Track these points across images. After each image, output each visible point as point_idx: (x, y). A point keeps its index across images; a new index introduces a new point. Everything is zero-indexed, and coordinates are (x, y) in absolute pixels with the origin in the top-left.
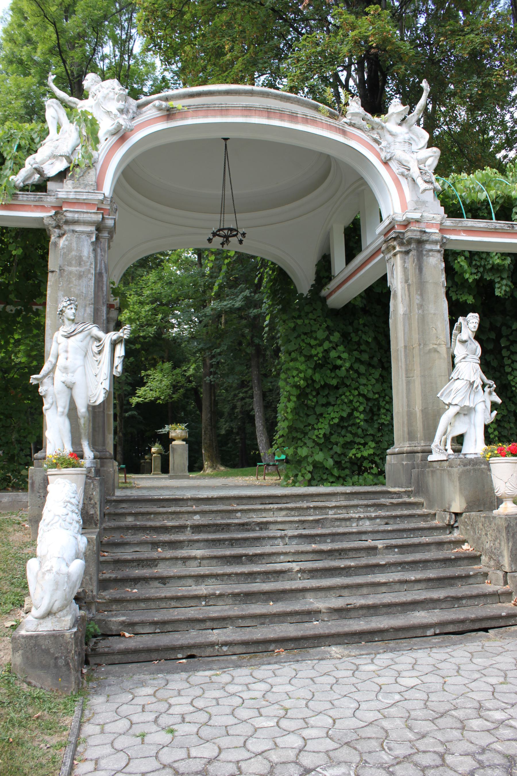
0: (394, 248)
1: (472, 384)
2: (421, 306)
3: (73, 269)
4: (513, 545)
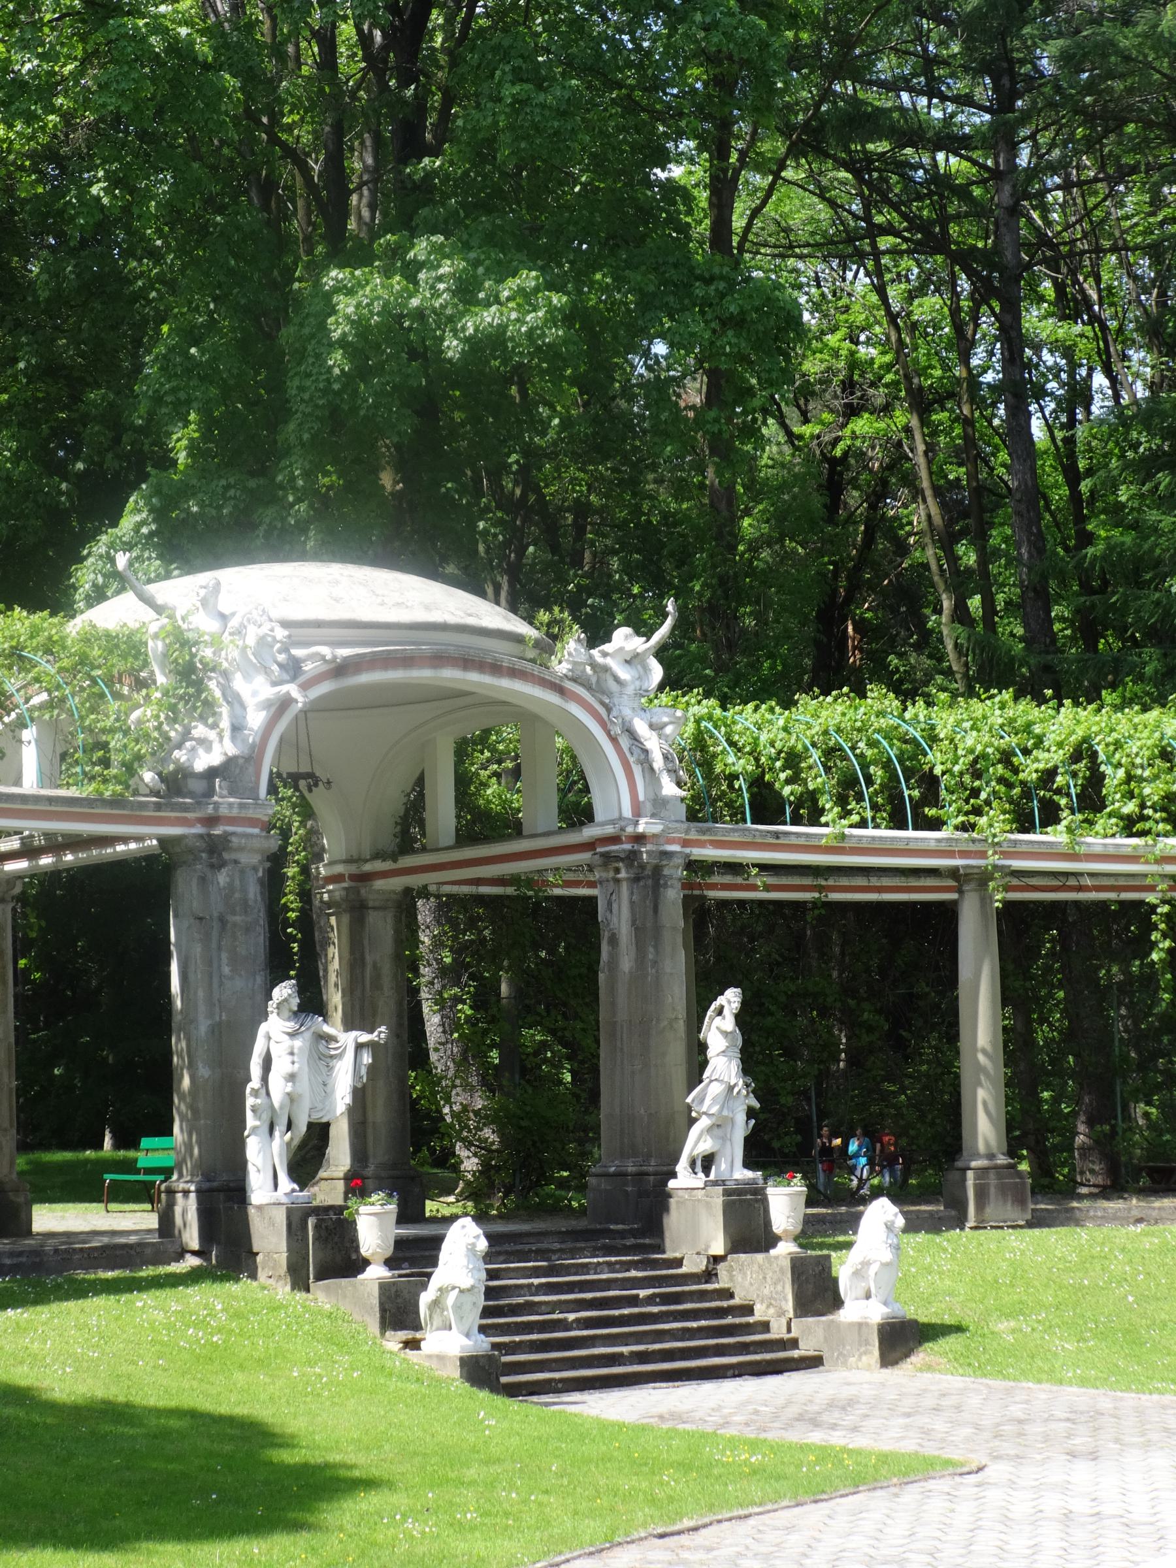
0: (617, 871)
1: (731, 1088)
3: (238, 918)
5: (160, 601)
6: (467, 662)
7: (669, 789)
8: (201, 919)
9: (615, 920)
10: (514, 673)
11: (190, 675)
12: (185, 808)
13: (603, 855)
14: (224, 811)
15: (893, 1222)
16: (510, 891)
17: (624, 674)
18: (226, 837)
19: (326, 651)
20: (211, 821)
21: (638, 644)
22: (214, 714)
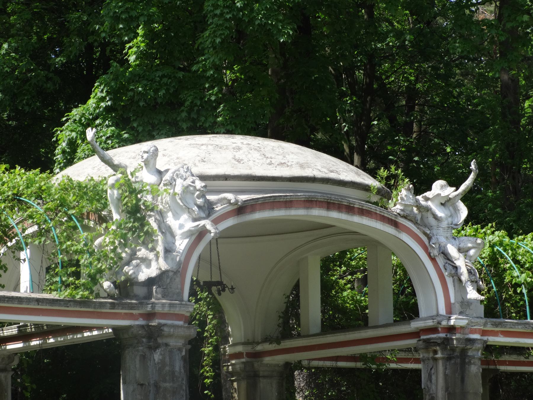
0: (435, 352)
3: (168, 385)
5: (116, 162)
6: (330, 204)
7: (472, 294)
8: (142, 385)
9: (434, 387)
10: (362, 212)
11: (136, 213)
12: (132, 307)
13: (425, 341)
14: (158, 309)
16: (359, 365)
17: (440, 213)
18: (160, 326)
19: (230, 196)
20: (150, 316)
21: (450, 192)
22: (153, 241)
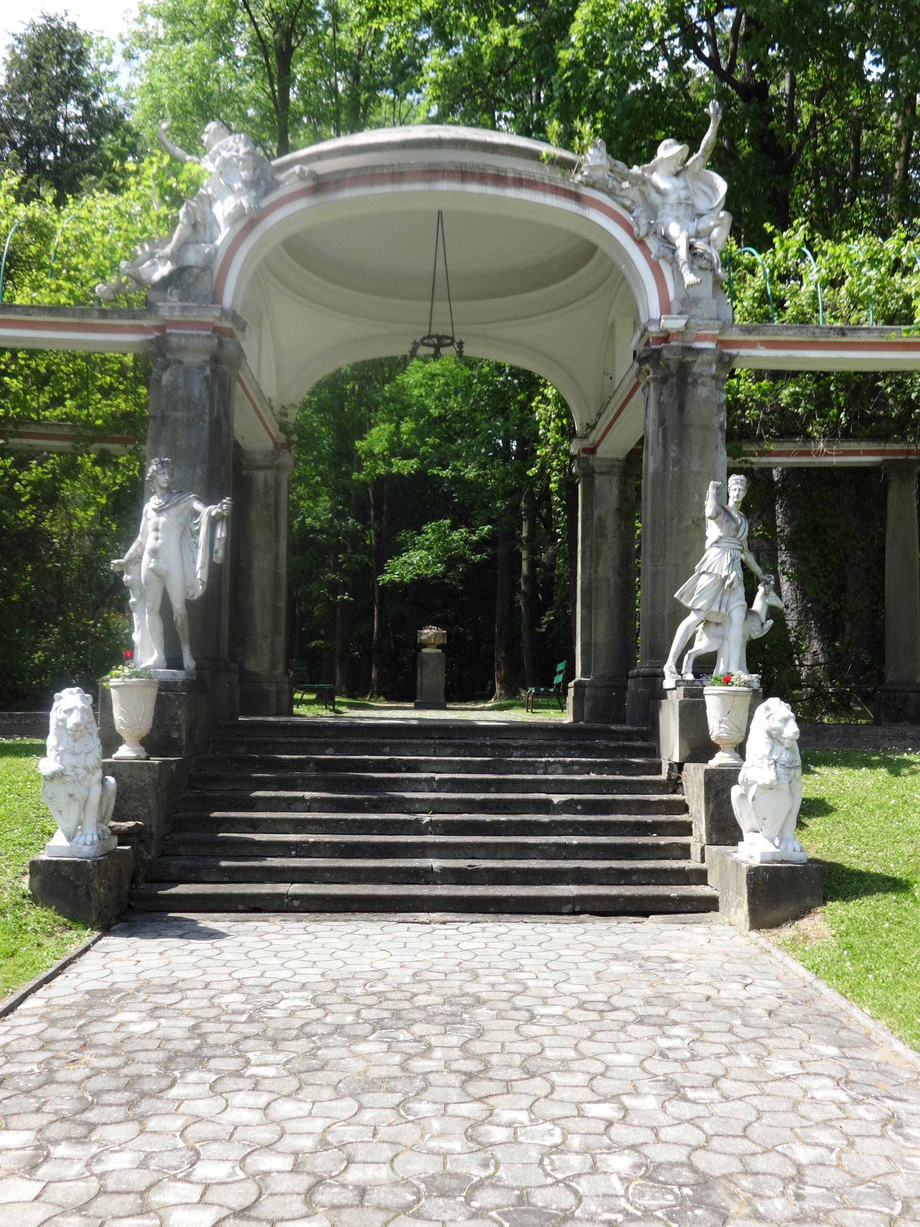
2: (678, 461)
3: (180, 414)
4: (716, 807)
15: (780, 732)
